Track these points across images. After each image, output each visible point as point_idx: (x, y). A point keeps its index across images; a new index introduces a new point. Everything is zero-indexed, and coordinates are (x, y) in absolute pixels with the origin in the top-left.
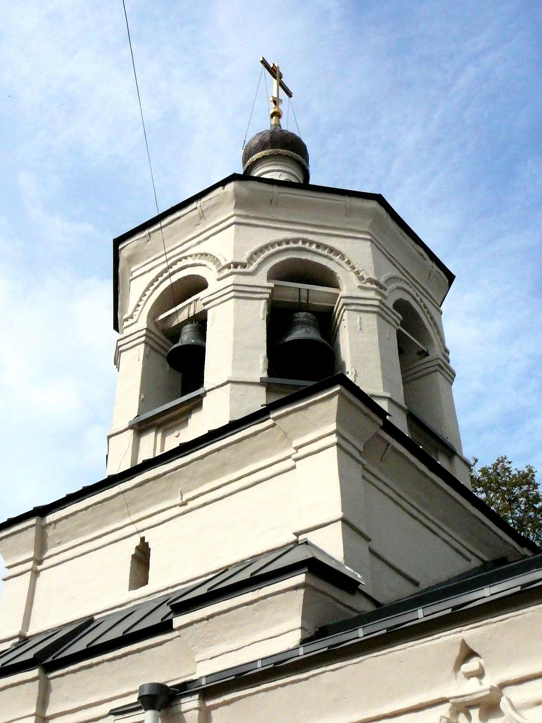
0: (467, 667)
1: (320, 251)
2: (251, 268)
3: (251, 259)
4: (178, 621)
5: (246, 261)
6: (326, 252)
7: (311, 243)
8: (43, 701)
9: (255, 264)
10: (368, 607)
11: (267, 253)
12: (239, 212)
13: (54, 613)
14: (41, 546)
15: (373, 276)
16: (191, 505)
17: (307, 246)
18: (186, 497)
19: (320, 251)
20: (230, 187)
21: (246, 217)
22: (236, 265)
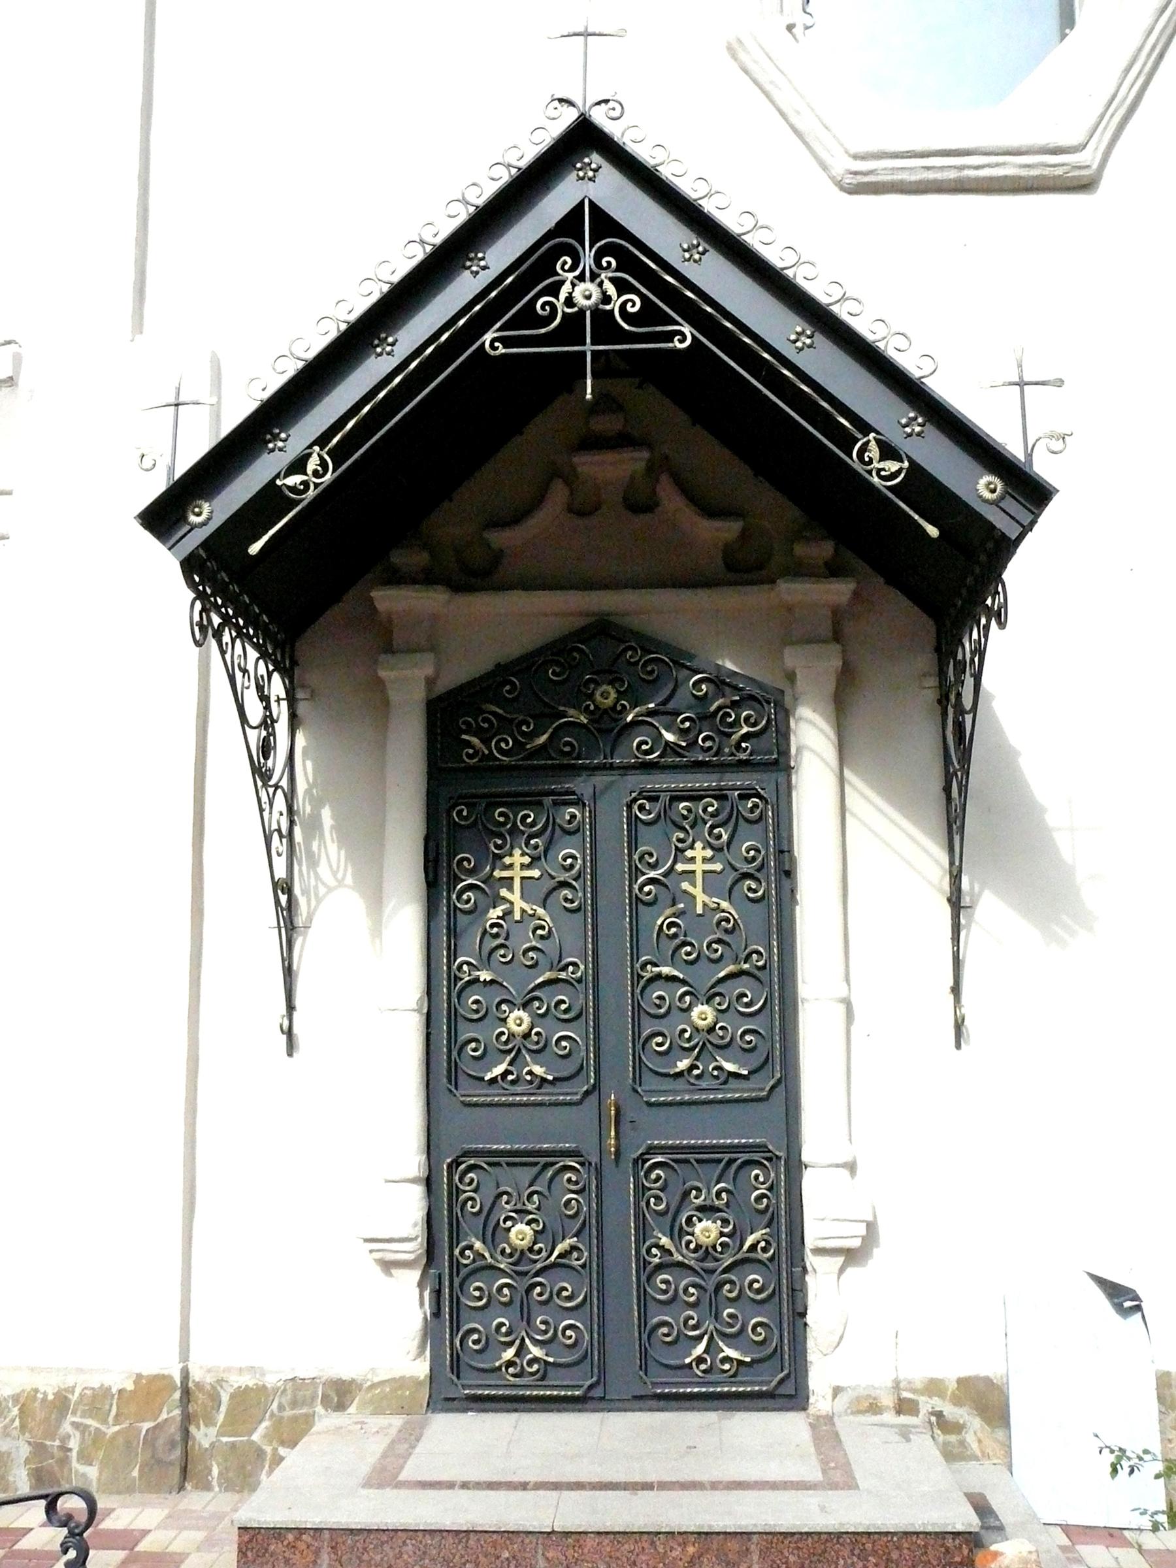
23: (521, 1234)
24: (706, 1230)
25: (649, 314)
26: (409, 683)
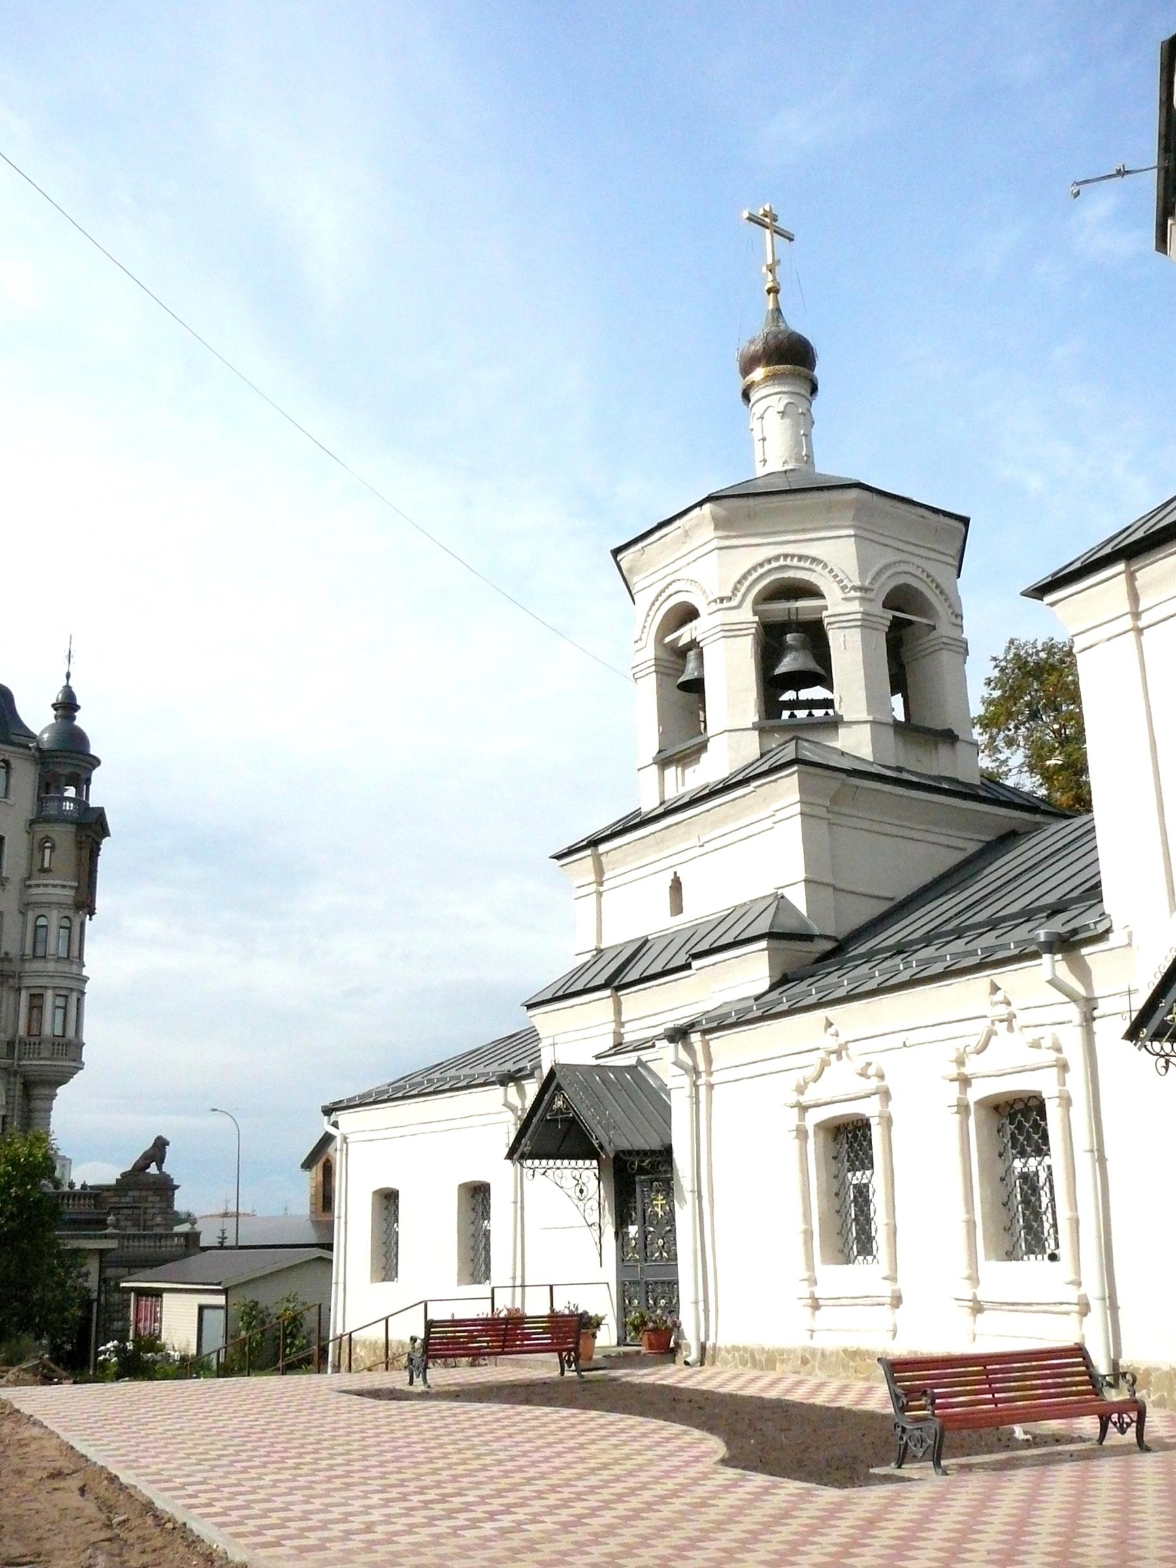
0: (831, 1030)
1: (802, 564)
2: (734, 603)
3: (735, 589)
4: (696, 964)
5: (730, 594)
6: (807, 565)
7: (793, 556)
8: (618, 1011)
9: (740, 595)
10: (828, 946)
11: (751, 579)
12: (720, 533)
13: (621, 932)
14: (600, 871)
15: (858, 583)
16: (708, 847)
17: (788, 562)
18: (703, 840)
19: (802, 564)
20: (707, 507)
21: (727, 537)
22: (722, 600)
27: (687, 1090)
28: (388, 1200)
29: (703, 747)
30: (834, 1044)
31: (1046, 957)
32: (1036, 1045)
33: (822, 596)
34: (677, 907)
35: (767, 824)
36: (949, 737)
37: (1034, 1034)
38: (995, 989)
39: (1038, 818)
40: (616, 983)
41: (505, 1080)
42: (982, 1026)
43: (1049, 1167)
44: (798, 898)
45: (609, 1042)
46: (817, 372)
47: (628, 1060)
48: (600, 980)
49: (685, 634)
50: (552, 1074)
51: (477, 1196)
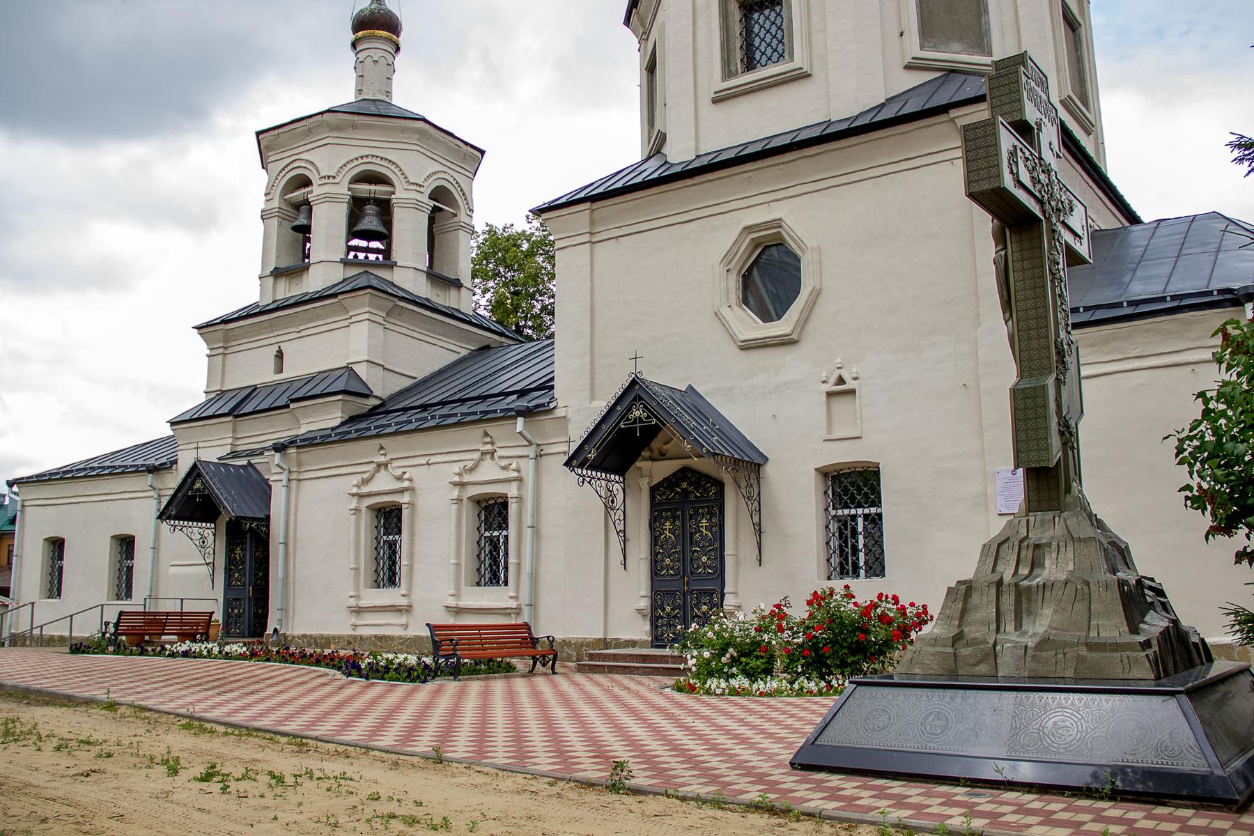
4: (292, 406)
23: (668, 609)
24: (704, 608)
25: (648, 417)
26: (645, 485)
27: (284, 483)
28: (57, 546)
29: (307, 268)
30: (382, 459)
31: (520, 420)
32: (504, 468)
33: (393, 186)
34: (279, 370)
35: (346, 323)
36: (457, 284)
37: (504, 463)
38: (486, 434)
39: (503, 339)
40: (236, 413)
41: (153, 470)
42: (476, 456)
43: (506, 537)
44: (361, 370)
45: (228, 449)
46: (402, 40)
47: (244, 462)
48: (225, 410)
49: (298, 194)
50: (195, 466)
51: (126, 544)
